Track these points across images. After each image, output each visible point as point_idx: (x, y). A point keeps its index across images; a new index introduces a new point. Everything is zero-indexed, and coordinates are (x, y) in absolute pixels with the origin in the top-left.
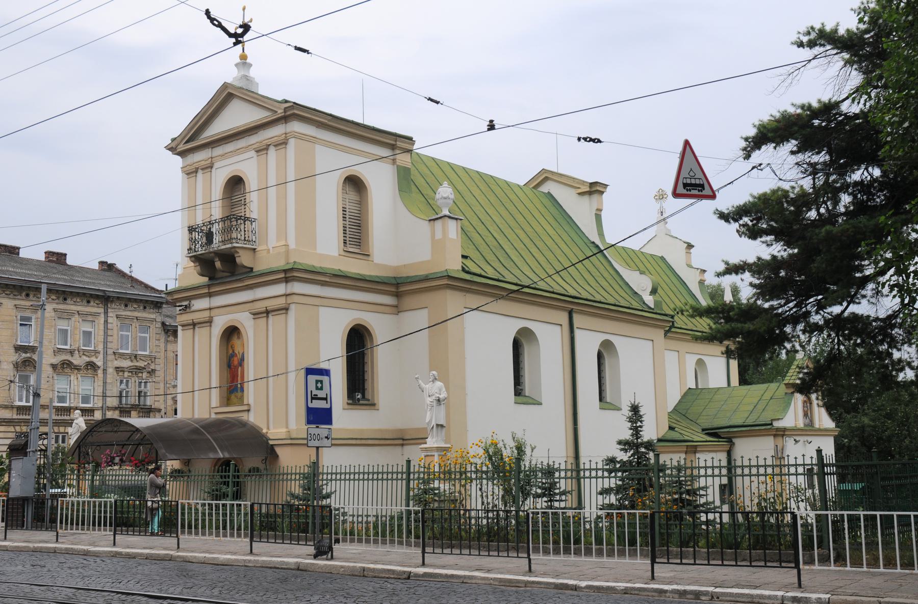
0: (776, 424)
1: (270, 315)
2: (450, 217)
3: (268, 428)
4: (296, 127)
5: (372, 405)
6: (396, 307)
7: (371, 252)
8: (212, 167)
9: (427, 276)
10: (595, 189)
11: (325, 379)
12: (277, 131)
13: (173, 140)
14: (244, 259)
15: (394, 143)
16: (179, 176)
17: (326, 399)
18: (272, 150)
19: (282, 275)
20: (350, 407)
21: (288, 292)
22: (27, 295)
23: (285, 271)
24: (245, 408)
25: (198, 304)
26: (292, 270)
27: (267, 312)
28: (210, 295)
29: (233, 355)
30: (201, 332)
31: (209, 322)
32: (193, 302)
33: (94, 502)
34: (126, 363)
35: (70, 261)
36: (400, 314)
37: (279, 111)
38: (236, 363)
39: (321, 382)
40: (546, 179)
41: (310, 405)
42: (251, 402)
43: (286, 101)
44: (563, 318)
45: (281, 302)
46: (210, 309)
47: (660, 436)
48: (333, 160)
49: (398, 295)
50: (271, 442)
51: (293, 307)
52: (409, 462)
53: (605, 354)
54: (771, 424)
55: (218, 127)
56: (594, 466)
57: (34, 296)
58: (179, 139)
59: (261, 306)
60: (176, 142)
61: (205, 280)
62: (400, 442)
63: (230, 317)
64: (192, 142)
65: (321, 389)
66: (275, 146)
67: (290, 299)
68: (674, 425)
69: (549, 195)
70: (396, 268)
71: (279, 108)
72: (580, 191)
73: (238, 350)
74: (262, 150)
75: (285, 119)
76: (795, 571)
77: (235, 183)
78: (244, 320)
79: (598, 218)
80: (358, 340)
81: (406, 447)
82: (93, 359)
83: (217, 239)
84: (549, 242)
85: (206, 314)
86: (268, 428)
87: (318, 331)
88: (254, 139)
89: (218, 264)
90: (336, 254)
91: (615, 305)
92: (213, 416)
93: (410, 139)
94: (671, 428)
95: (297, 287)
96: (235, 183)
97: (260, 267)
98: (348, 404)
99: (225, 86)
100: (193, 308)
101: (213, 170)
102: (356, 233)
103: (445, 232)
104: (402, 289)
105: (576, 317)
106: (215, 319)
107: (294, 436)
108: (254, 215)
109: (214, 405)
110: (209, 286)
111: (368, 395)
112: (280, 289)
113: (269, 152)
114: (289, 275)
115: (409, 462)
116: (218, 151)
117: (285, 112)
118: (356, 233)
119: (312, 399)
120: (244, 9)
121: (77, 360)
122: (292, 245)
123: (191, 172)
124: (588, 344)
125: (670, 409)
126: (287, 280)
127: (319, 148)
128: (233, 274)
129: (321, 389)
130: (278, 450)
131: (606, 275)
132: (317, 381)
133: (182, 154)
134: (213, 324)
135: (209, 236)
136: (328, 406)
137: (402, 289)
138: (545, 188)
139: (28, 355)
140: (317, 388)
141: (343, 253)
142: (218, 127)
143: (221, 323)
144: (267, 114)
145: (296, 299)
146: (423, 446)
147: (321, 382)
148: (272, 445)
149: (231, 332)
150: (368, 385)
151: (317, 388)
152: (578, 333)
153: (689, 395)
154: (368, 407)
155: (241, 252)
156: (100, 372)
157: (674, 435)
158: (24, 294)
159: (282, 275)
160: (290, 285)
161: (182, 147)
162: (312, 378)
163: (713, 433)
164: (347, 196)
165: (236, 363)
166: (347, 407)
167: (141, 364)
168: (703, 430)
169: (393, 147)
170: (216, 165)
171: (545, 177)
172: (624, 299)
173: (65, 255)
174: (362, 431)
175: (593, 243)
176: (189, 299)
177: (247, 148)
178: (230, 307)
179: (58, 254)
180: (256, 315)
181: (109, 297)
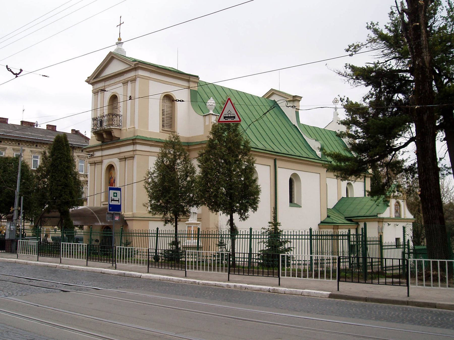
0: (379, 216)
1: (127, 161)
2: (213, 114)
3: (124, 212)
4: (141, 73)
9: (201, 142)
10: (296, 99)
11: (118, 192)
12: (131, 75)
13: (88, 78)
14: (116, 134)
15: (189, 78)
16: (91, 94)
17: (118, 201)
18: (129, 84)
19: (131, 142)
21: (134, 149)
22: (37, 146)
23: (133, 140)
25: (98, 154)
26: (135, 139)
27: (125, 158)
28: (102, 150)
29: (112, 178)
30: (98, 167)
31: (101, 162)
32: (95, 153)
33: (65, 244)
35: (57, 130)
37: (133, 65)
38: (112, 182)
39: (116, 193)
40: (273, 94)
41: (110, 203)
44: (271, 162)
45: (131, 153)
46: (102, 156)
47: (322, 220)
48: (157, 88)
50: (125, 219)
51: (136, 156)
52: (158, 229)
53: (294, 180)
54: (377, 216)
55: (109, 71)
56: (301, 234)
59: (122, 155)
60: (89, 79)
63: (110, 160)
64: (97, 79)
65: (116, 196)
66: (131, 81)
67: (135, 153)
68: (330, 215)
69: (275, 102)
70: (188, 138)
71: (132, 64)
72: (288, 100)
74: (125, 83)
75: (135, 69)
76: (407, 287)
77: (114, 98)
78: (115, 161)
79: (297, 114)
83: (105, 124)
84: (270, 125)
85: (100, 159)
86: (124, 212)
89: (105, 136)
91: (299, 156)
92: (102, 206)
93: (198, 77)
94: (328, 217)
95: (138, 147)
96: (114, 98)
97: (123, 137)
99: (111, 53)
100: (95, 156)
104: (190, 148)
105: (279, 163)
106: (104, 161)
107: (135, 216)
109: (102, 201)
110: (101, 146)
112: (130, 148)
114: (134, 141)
115: (158, 229)
116: (108, 83)
117: (135, 66)
119: (112, 200)
122: (137, 128)
123: (95, 93)
124: (284, 175)
125: (331, 206)
126: (134, 144)
127: (151, 82)
128: (112, 140)
129: (116, 196)
130: (128, 223)
131: (298, 141)
132: (114, 193)
133: (92, 84)
134: (103, 164)
135: (101, 122)
136: (120, 204)
137: (190, 148)
138: (272, 98)
140: (114, 196)
141: (162, 131)
142: (109, 71)
143: (106, 163)
144: (128, 66)
145: (137, 152)
146: (187, 222)
147: (116, 193)
149: (111, 167)
151: (114, 196)
152: (279, 170)
153: (341, 201)
155: (114, 130)
157: (329, 220)
158: (35, 145)
159: (131, 142)
160: (135, 146)
161: (92, 81)
162: (112, 192)
163: (350, 219)
164: (165, 104)
165: (112, 182)
168: (345, 218)
169: (188, 81)
171: (273, 92)
172: (305, 153)
173: (55, 127)
175: (294, 125)
176: (93, 151)
177: (119, 82)
178: (110, 156)
179: (52, 126)
180: (121, 159)
181: (74, 147)
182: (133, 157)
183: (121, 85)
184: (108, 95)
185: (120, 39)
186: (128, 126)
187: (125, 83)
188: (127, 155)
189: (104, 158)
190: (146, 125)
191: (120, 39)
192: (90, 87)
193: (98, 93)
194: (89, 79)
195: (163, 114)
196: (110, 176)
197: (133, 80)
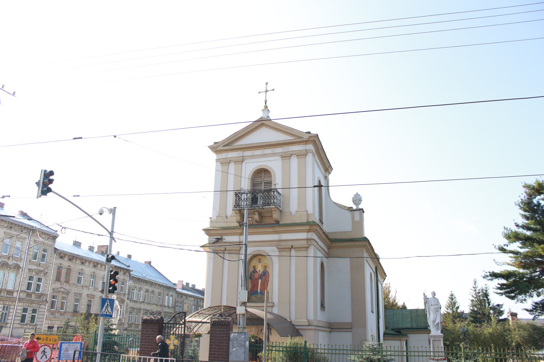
8: (242, 162)
13: (215, 143)
21: (309, 237)
24: (272, 305)
25: (228, 239)
29: (255, 271)
34: (34, 267)
42: (276, 300)
43: (309, 133)
50: (297, 327)
58: (220, 144)
61: (237, 224)
63: (257, 248)
66: (297, 156)
73: (260, 269)
74: (286, 157)
81: (332, 333)
82: (19, 263)
88: (279, 150)
101: (244, 164)
113: (292, 158)
116: (248, 153)
120: (267, 84)
121: (11, 262)
123: (224, 163)
148: (297, 330)
156: (21, 270)
167: (41, 269)
170: (246, 161)
177: (274, 154)
180: (281, 249)
183: (278, 158)
184: (250, 167)
185: (266, 107)
187: (286, 157)
188: (295, 244)
191: (266, 107)
193: (229, 163)
194: (217, 145)
196: (251, 269)
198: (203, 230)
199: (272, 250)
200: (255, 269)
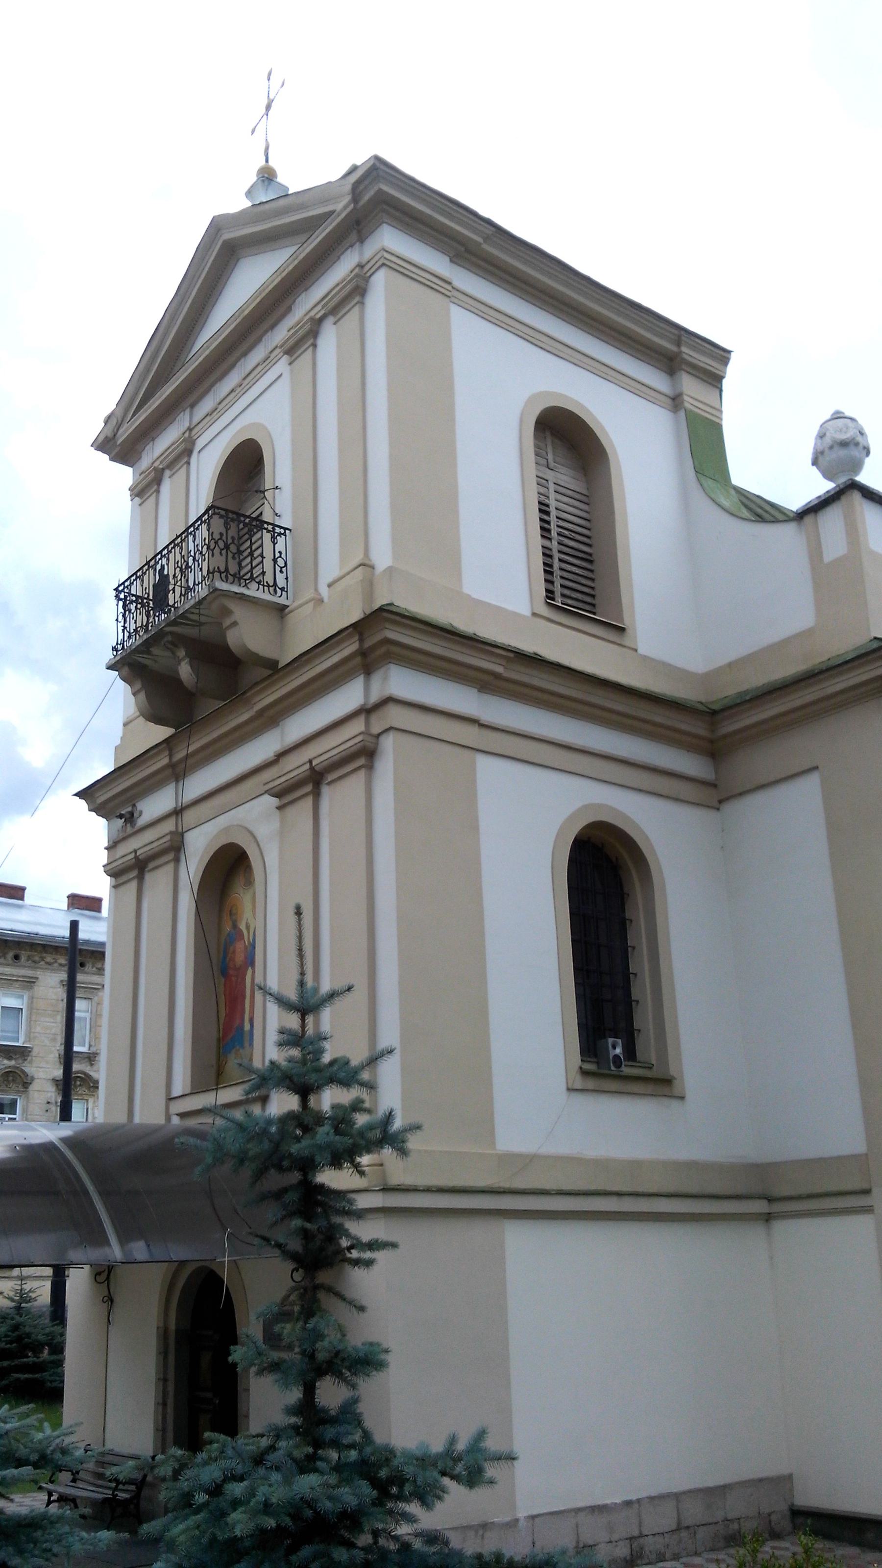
5: (662, 1084)
6: (713, 785)
7: (627, 623)
14: (248, 634)
20: (591, 1083)
21: (374, 698)
22: (17, 957)
23: (358, 628)
36: (727, 808)
38: (240, 958)
48: (502, 374)
49: (714, 750)
51: (388, 743)
57: (29, 958)
61: (163, 732)
62: (760, 1207)
63: (222, 821)
80: (602, 879)
81: (779, 1226)
87: (474, 827)
90: (527, 612)
95: (400, 682)
98: (584, 1073)
99: (217, 226)
102: (579, 566)
103: (854, 533)
104: (729, 727)
108: (285, 521)
109: (177, 1091)
111: (647, 1048)
118: (579, 566)
122: (382, 557)
123: (145, 490)
126: (367, 663)
139: (13, 1063)
141: (544, 611)
145: (395, 716)
150: (644, 1019)
154: (650, 1088)
155: (239, 612)
158: (11, 954)
164: (549, 475)
166: (579, 1083)
174: (635, 1165)
177: (267, 362)
182: (365, 755)
186: (330, 566)
189: (189, 817)
190: (451, 558)
192: (125, 475)
195: (545, 531)
197: (356, 290)
198: (80, 794)
199: (256, 820)
200: (235, 926)
